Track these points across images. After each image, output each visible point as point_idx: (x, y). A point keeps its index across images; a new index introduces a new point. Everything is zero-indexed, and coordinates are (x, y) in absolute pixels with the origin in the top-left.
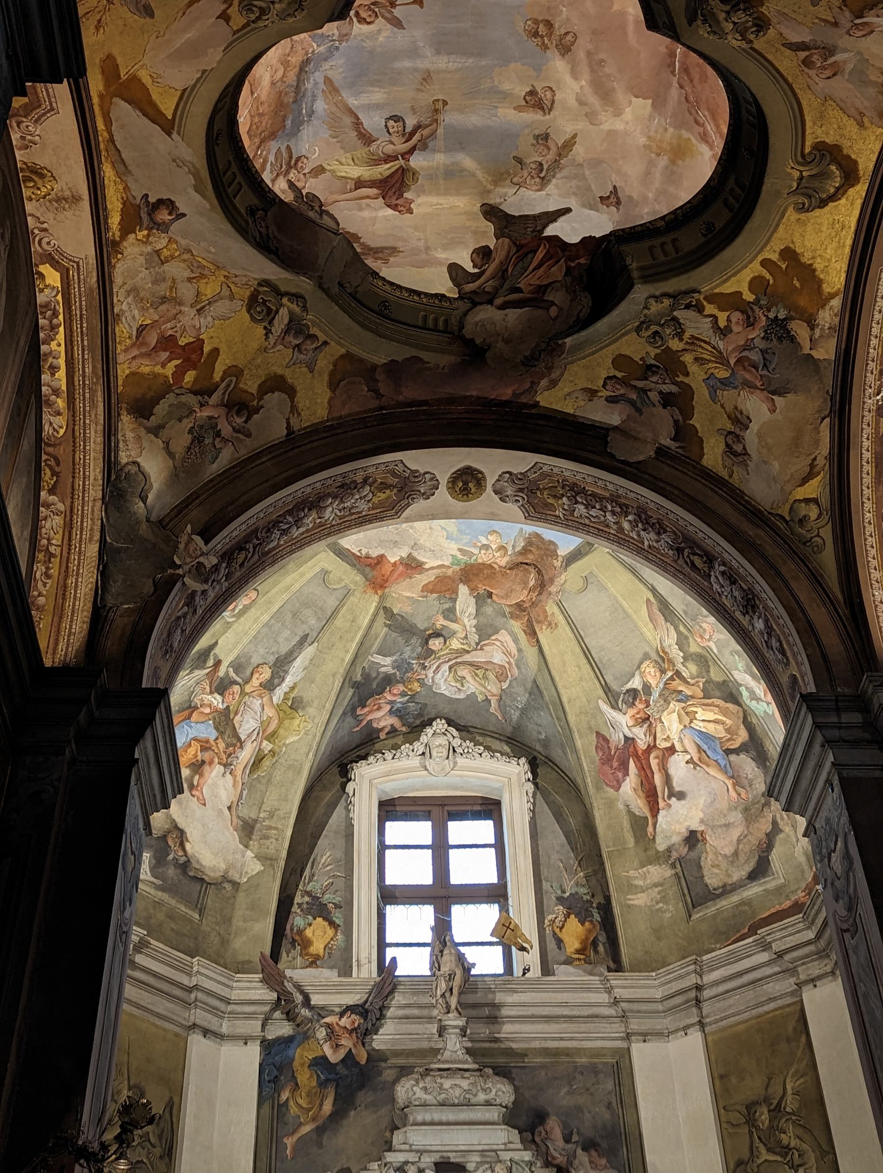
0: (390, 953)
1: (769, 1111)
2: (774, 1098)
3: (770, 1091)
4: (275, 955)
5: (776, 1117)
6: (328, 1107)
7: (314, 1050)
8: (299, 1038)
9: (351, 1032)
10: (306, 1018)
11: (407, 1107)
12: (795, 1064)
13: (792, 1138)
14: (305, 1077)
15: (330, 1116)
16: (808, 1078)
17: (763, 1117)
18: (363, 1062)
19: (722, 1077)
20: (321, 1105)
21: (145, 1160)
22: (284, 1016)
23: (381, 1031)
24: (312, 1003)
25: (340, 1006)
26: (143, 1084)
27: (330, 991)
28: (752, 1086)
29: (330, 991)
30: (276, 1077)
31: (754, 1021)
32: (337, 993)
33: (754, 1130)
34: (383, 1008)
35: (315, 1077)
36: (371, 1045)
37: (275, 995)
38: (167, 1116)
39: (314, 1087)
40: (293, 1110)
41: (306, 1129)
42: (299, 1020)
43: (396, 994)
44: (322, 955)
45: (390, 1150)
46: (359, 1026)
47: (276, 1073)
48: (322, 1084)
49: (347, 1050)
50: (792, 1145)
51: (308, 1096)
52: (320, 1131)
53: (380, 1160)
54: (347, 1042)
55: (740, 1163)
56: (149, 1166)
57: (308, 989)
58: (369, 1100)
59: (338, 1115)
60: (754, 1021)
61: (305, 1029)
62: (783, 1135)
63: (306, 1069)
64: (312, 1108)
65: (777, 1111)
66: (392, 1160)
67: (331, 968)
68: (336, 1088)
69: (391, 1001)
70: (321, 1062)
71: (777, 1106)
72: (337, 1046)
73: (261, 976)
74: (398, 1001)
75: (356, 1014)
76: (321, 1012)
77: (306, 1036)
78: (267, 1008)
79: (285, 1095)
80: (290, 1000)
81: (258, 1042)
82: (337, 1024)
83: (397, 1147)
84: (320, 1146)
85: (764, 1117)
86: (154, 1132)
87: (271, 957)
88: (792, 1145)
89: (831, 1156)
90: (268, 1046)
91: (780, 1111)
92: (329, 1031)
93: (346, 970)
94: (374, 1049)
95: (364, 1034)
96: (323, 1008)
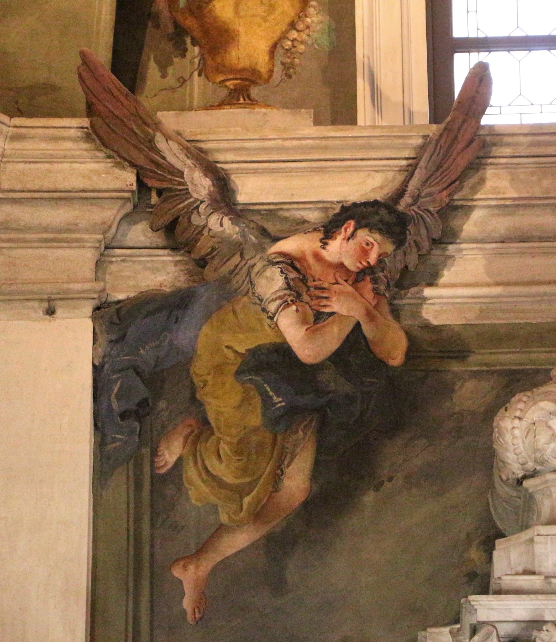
0: (462, 65)
4: (127, 64)
6: (297, 481)
7: (253, 330)
8: (205, 295)
9: (356, 278)
10: (224, 240)
11: (534, 474)
14: (228, 403)
15: (305, 504)
18: (397, 358)
20: (277, 478)
22: (158, 239)
23: (447, 276)
24: (241, 198)
25: (322, 205)
27: (290, 169)
29: (290, 169)
30: (144, 403)
32: (312, 170)
34: (451, 211)
35: (257, 401)
36: (416, 314)
37: (129, 178)
39: (256, 430)
41: (239, 541)
42: (204, 246)
43: (489, 172)
44: (263, 68)
45: (484, 590)
46: (380, 260)
47: (141, 391)
48: (281, 421)
51: (238, 452)
53: (457, 621)
54: (346, 306)
57: (225, 158)
58: (417, 462)
59: (328, 503)
63: (230, 380)
64: (251, 486)
66: (493, 616)
67: (294, 105)
68: (320, 430)
69: (475, 189)
70: (274, 361)
72: (319, 316)
73: (85, 122)
74: (495, 190)
75: (371, 227)
76: (268, 224)
77: (228, 292)
78: (110, 213)
79: (171, 453)
81: (88, 308)
82: (318, 257)
83: (508, 581)
84: (278, 585)
87: (114, 70)
90: (116, 320)
92: (293, 275)
93: (340, 109)
94: (427, 326)
96: (272, 212)
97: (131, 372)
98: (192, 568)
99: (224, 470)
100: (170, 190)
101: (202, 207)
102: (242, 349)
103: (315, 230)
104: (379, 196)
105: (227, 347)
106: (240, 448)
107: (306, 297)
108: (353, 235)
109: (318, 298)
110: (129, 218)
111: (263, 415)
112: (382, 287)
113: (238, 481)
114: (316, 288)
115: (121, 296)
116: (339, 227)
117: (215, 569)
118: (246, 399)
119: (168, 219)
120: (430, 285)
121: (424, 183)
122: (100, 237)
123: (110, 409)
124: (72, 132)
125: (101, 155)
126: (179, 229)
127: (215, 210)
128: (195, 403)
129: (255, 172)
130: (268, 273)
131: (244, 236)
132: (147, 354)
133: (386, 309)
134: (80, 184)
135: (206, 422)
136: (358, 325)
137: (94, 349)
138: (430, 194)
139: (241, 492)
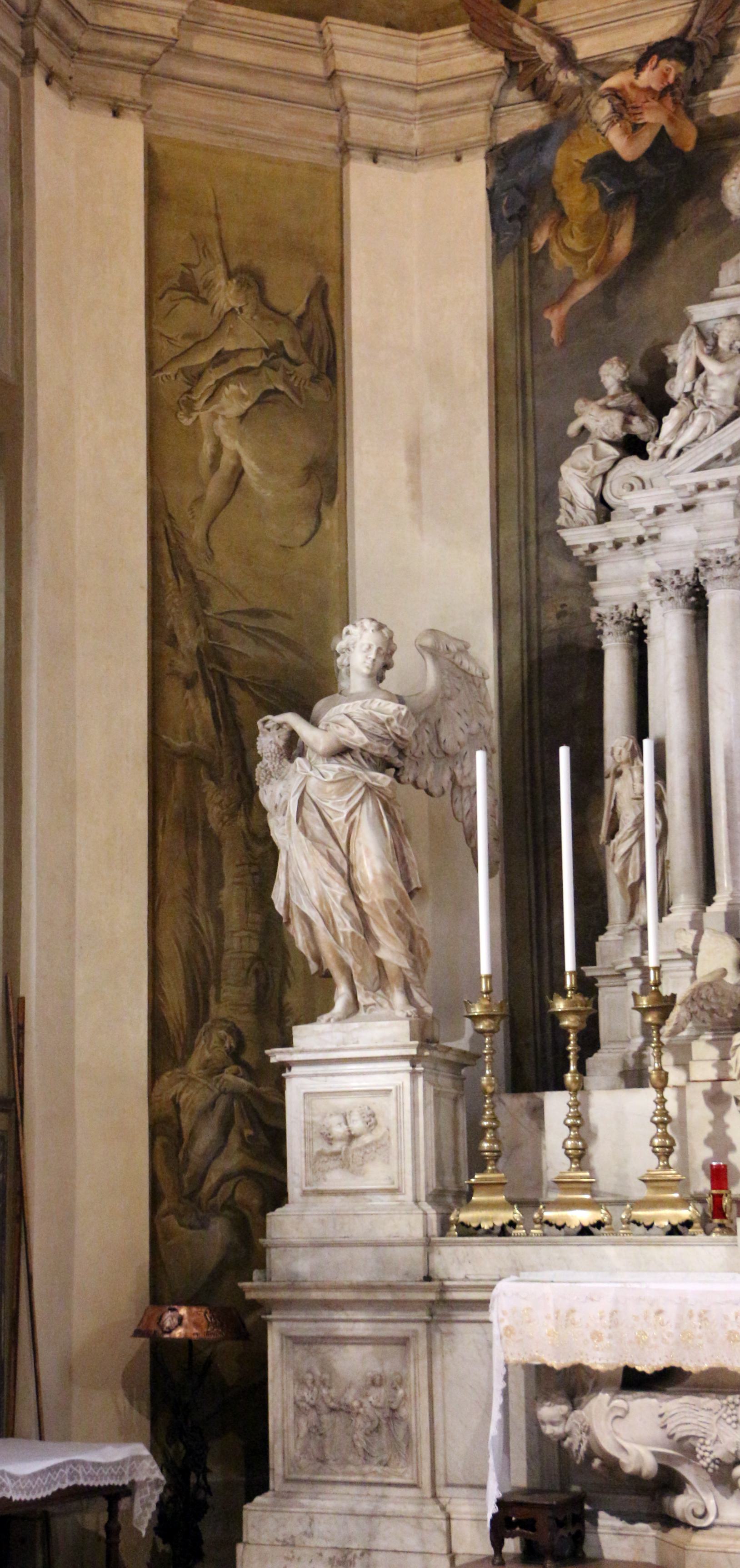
6: (623, 243)
10: (571, 88)
15: (629, 258)
21: (281, 387)
22: (526, 94)
26: (256, 263)
30: (523, 208)
32: (628, 25)
35: (596, 194)
38: (317, 309)
39: (596, 212)
40: (559, 259)
41: (585, 289)
42: (556, 94)
46: (677, 79)
47: (521, 200)
48: (611, 205)
49: (656, 130)
52: (611, 288)
56: (292, 396)
58: (703, 215)
59: (643, 254)
61: (571, 107)
64: (593, 251)
68: (638, 205)
70: (607, 164)
76: (596, 70)
80: (532, 61)
81: (482, 152)
86: (293, 341)
90: (501, 157)
92: (617, 102)
95: (686, 94)
96: (602, 61)
97: (514, 189)
98: (556, 312)
99: (576, 244)
100: (529, 61)
101: (552, 68)
102: (584, 160)
103: (630, 67)
104: (674, 34)
105: (577, 161)
106: (588, 227)
107: (626, 116)
108: (656, 66)
109: (635, 114)
110: (506, 85)
111: (600, 201)
112: (679, 98)
113: (585, 249)
114: (633, 108)
115: (505, 139)
116: (647, 62)
117: (573, 308)
118: (589, 194)
119: (530, 79)
120: (716, 87)
121: (705, 17)
122: (487, 102)
123: (501, 215)
124: (460, 36)
125: (480, 47)
126: (538, 86)
127: (562, 68)
128: (556, 203)
129: (589, 35)
130: (600, 104)
131: (582, 81)
132: (523, 175)
133: (682, 112)
134: (468, 69)
135: (563, 215)
136: (663, 129)
137: (487, 179)
138: (710, 24)
139: (587, 255)
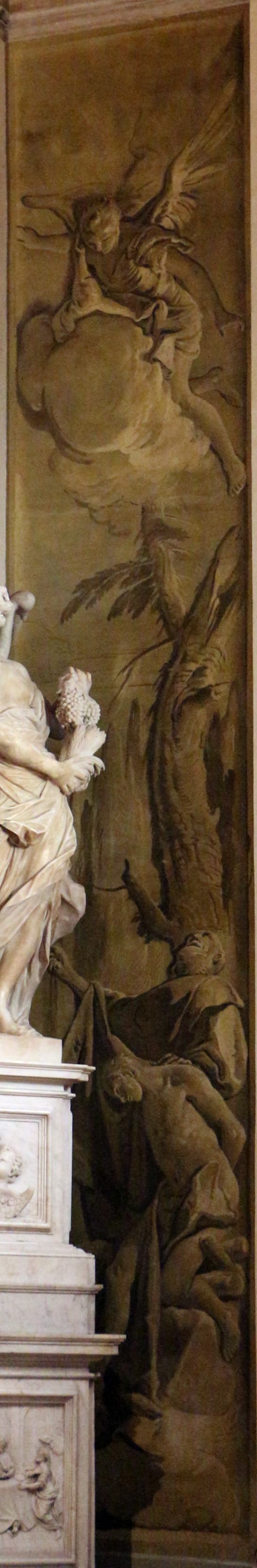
1: (124, 220)
2: (139, 196)
3: (133, 180)
5: (136, 234)
12: (201, 136)
13: (163, 279)
16: (223, 167)
17: (107, 230)
19: (29, 138)
28: (96, 164)
31: (127, 34)
33: (82, 251)
50: (161, 290)
55: (38, 309)
60: (127, 34)
62: (143, 272)
65: (141, 222)
71: (140, 215)
85: (109, 229)
88: (161, 290)
89: (235, 325)
91: (147, 223)
